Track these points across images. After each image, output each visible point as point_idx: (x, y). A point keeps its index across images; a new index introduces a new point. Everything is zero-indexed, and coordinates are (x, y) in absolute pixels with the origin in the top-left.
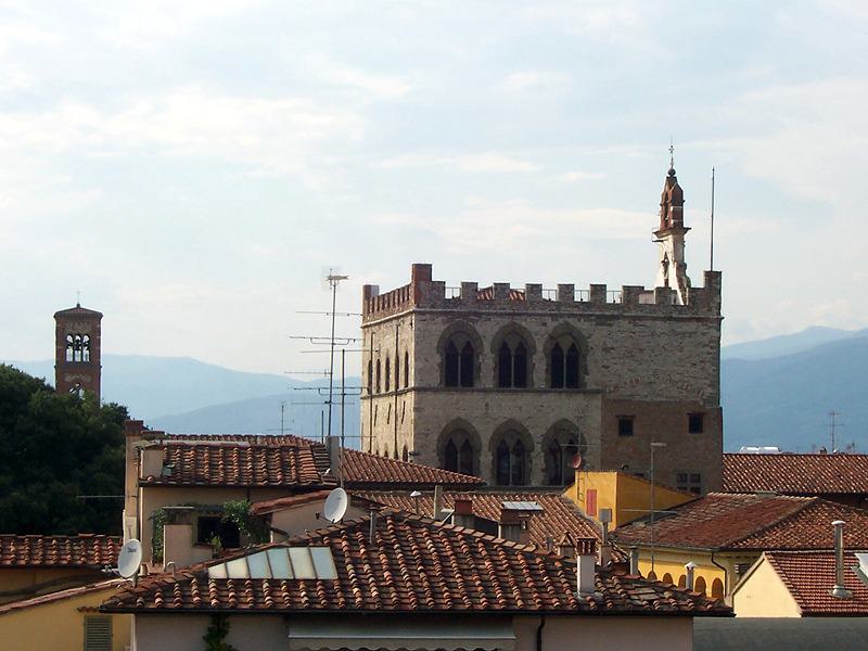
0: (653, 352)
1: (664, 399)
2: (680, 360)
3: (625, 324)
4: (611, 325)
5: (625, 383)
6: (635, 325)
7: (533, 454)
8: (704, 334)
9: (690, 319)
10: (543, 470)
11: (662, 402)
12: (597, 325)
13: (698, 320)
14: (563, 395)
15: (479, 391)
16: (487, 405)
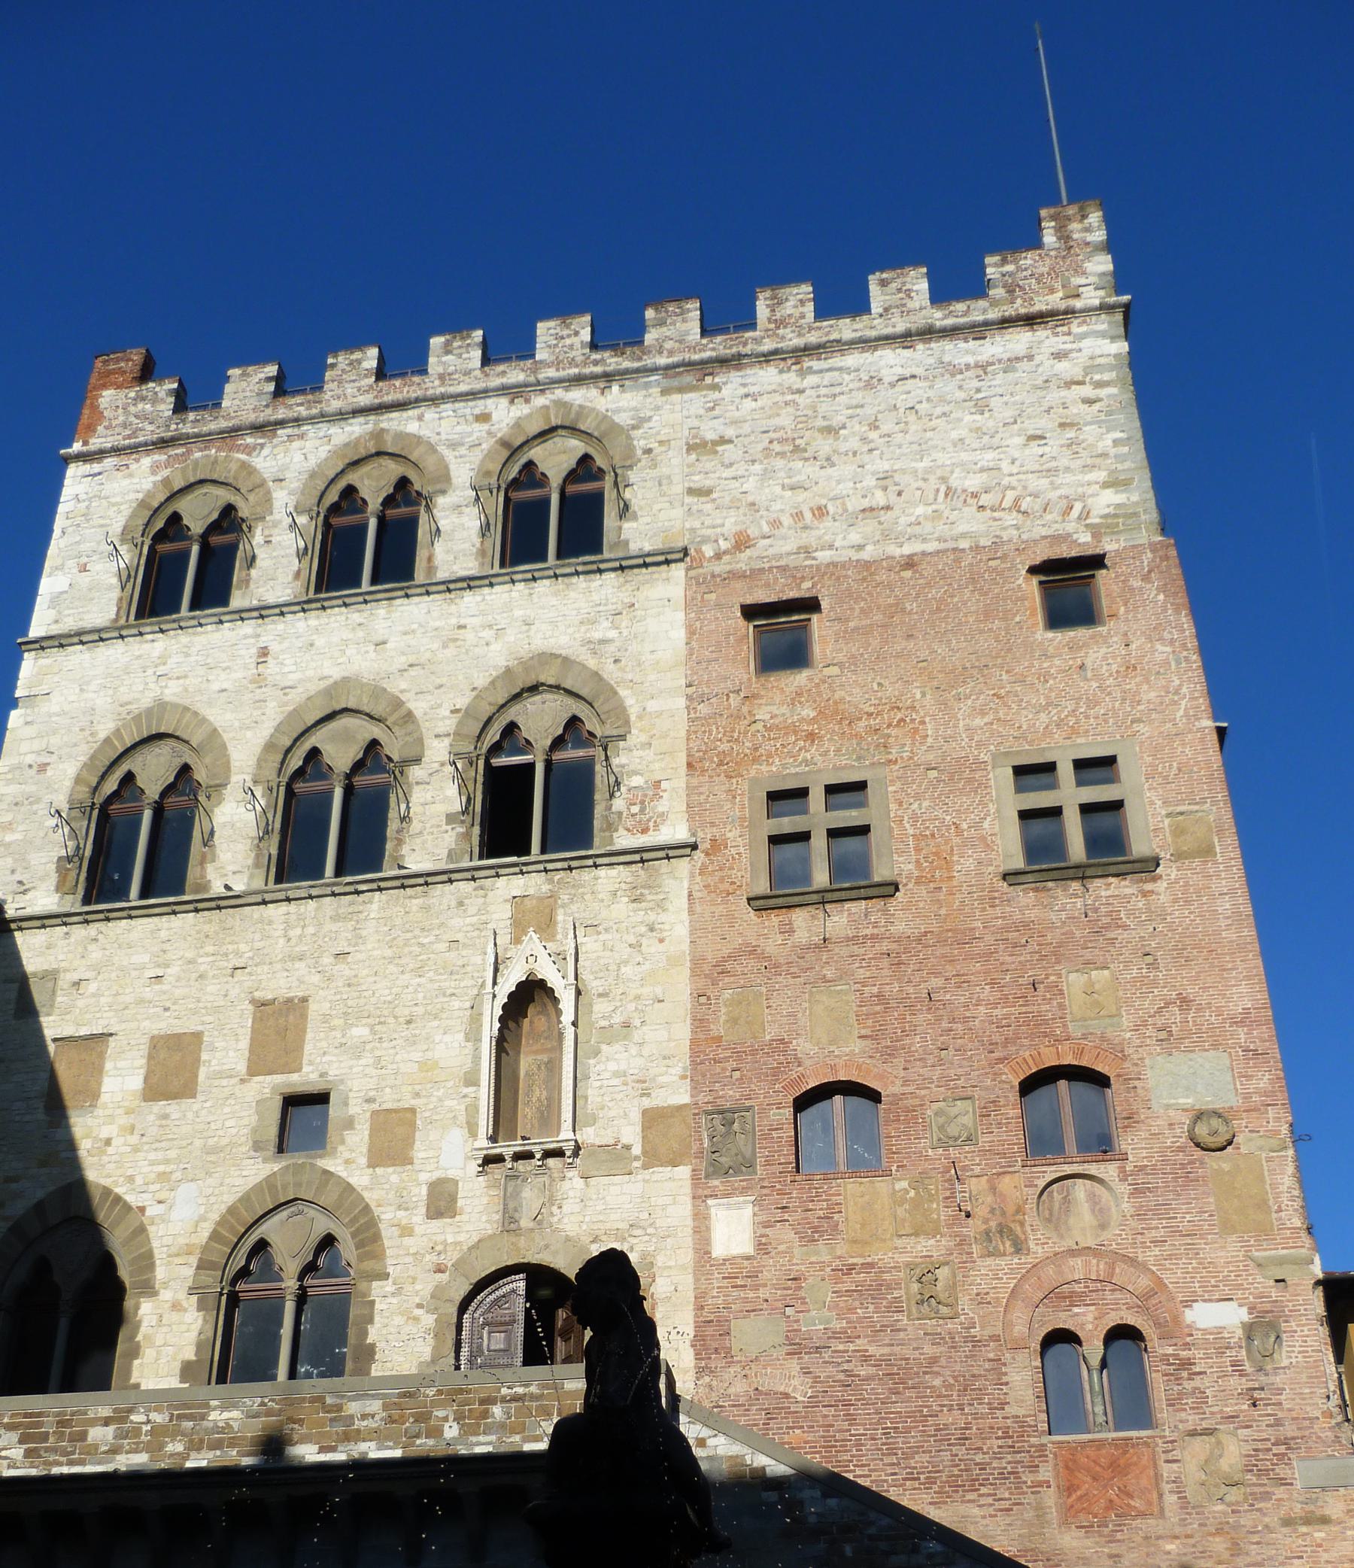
0: (874, 426)
1: (931, 547)
2: (978, 431)
4: (716, 387)
5: (776, 524)
6: (803, 373)
7: (415, 773)
8: (1059, 356)
9: (1006, 323)
10: (450, 818)
11: (924, 553)
12: (665, 392)
13: (1031, 320)
14: (543, 586)
15: (241, 615)
16: (264, 652)
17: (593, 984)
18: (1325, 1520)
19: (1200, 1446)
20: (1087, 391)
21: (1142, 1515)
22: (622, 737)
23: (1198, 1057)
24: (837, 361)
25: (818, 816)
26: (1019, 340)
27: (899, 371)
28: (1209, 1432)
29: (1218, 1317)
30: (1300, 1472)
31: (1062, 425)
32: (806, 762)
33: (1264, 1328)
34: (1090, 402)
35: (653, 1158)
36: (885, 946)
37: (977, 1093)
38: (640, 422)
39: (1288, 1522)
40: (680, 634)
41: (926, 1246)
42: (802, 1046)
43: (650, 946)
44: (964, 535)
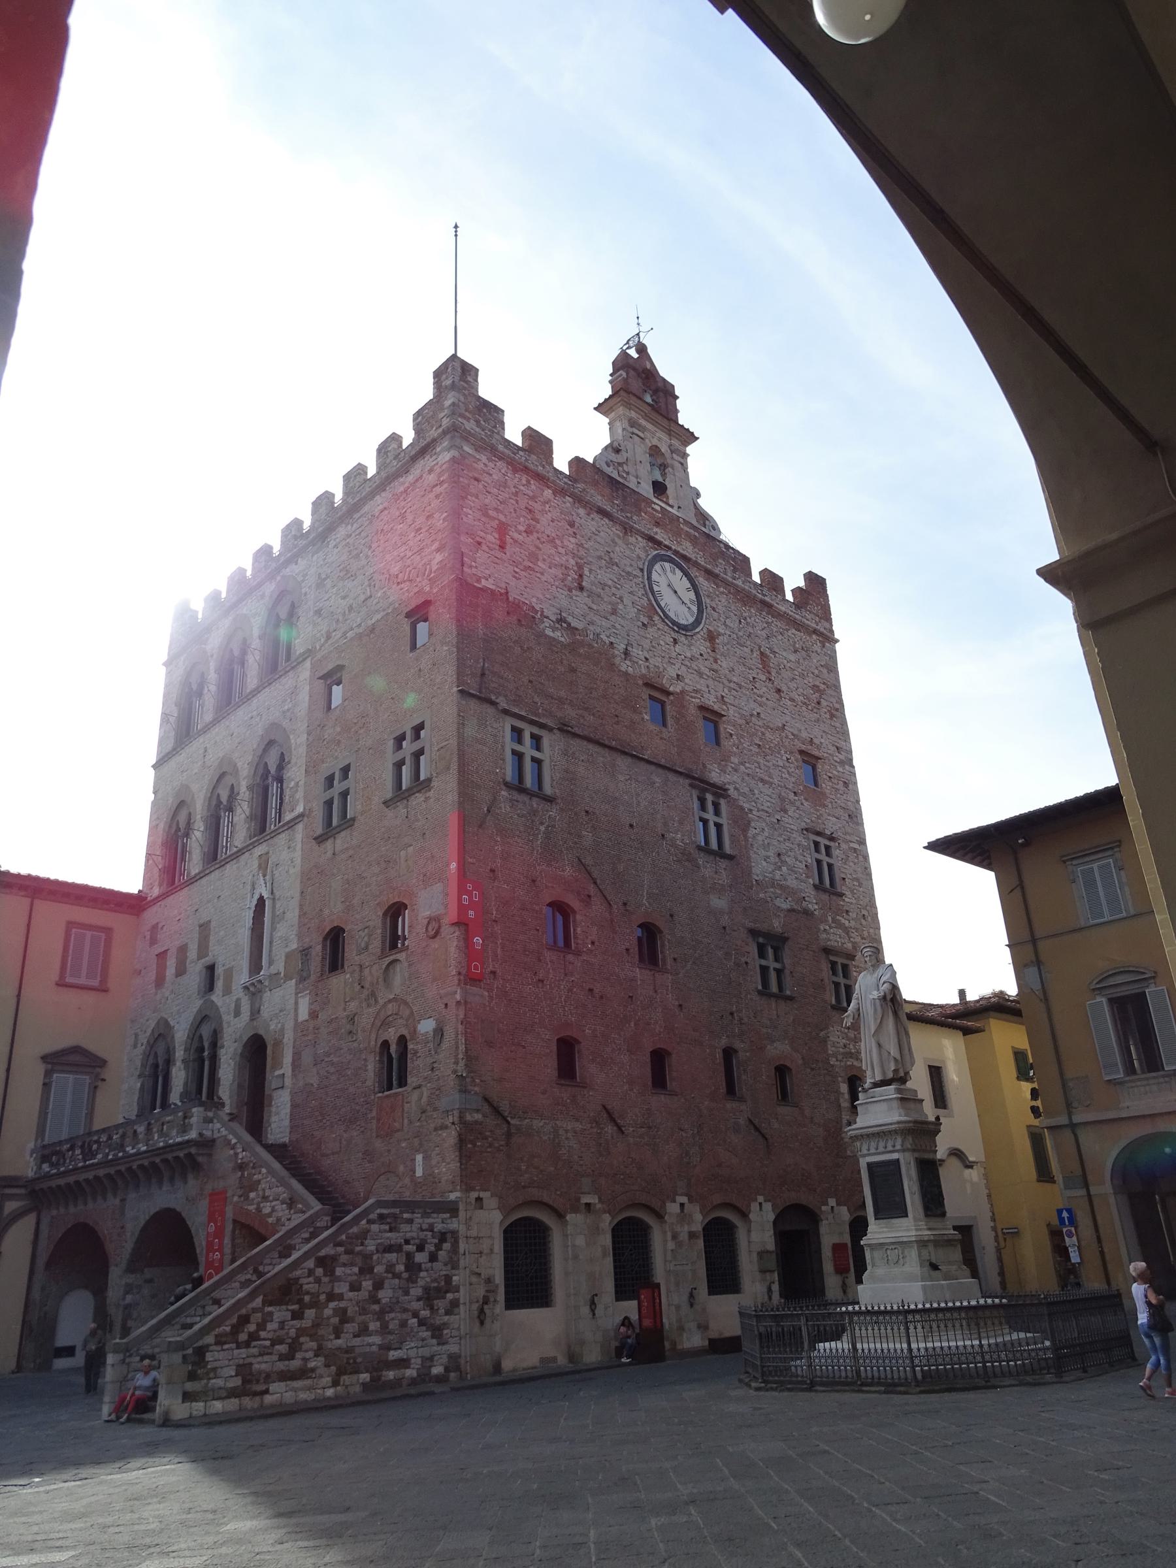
1: (379, 616)
2: (401, 535)
3: (342, 531)
11: (378, 621)
17: (277, 894)
18: (446, 1127)
19: (417, 1092)
20: (438, 490)
21: (398, 1131)
22: (289, 762)
24: (362, 512)
25: (338, 787)
26: (421, 463)
27: (381, 507)
28: (419, 1087)
29: (426, 1026)
31: (428, 517)
32: (337, 758)
33: (439, 1032)
34: (437, 497)
35: (288, 977)
36: (351, 852)
37: (371, 923)
39: (436, 1129)
40: (307, 698)
41: (353, 1006)
42: (326, 912)
44: (391, 604)
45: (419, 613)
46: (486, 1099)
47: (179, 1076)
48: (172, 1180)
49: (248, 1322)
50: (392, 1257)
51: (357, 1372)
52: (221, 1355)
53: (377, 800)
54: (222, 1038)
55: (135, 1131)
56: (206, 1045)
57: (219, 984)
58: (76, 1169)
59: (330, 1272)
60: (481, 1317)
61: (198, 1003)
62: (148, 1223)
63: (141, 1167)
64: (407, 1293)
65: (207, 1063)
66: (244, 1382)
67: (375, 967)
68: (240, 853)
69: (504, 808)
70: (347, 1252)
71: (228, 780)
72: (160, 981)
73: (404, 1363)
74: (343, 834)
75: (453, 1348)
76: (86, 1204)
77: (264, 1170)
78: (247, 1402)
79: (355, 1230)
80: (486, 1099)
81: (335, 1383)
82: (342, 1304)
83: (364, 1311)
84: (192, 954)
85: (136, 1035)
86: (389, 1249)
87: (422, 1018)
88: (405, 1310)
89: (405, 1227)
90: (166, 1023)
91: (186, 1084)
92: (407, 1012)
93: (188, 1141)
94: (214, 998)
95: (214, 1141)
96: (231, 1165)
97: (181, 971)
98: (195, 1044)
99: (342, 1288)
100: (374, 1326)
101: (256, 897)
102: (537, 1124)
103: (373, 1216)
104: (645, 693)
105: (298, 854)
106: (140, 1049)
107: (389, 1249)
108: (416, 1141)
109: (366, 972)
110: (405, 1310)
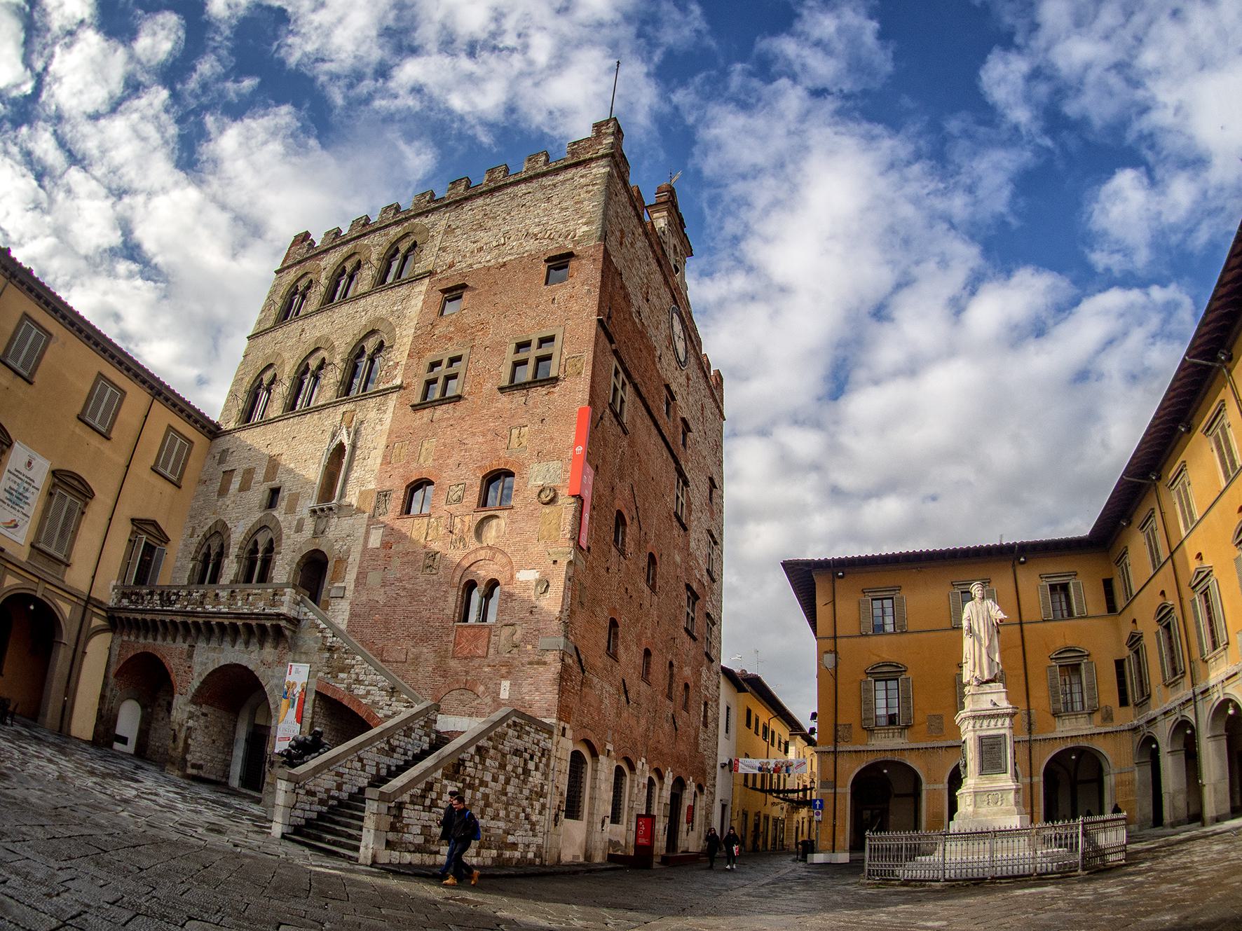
3: (480, 202)
17: (359, 444)
18: (545, 663)
23: (551, 464)
29: (528, 576)
30: (543, 643)
36: (452, 422)
38: (433, 225)
39: (530, 663)
43: (378, 427)
45: (560, 263)
46: (576, 649)
47: (231, 568)
48: (247, 643)
49: (431, 789)
50: (516, 759)
51: (490, 848)
52: (412, 814)
53: (490, 386)
54: (280, 546)
55: (217, 595)
56: (261, 549)
57: (282, 505)
58: (153, 611)
59: (483, 761)
60: (556, 820)
61: (257, 516)
62: (215, 671)
63: (220, 625)
64: (521, 792)
65: (259, 563)
66: (426, 841)
67: (467, 519)
68: (324, 407)
69: (607, 423)
70: (495, 748)
71: (323, 354)
72: (223, 491)
73: (514, 846)
74: (444, 407)
75: (540, 841)
76: (155, 639)
77: (359, 658)
78: (426, 856)
79: (499, 729)
80: (576, 649)
81: (478, 854)
82: (487, 791)
83: (498, 800)
84: (259, 475)
85: (194, 529)
86: (517, 752)
87: (521, 568)
88: (519, 805)
89: (526, 738)
90: (225, 525)
91: (236, 575)
92: (505, 560)
93: (278, 615)
94: (275, 513)
95: (299, 621)
96: (317, 646)
97: (244, 487)
98: (250, 546)
99: (488, 778)
100: (502, 813)
101: (337, 442)
102: (596, 680)
103: (510, 722)
104: (665, 392)
105: (388, 417)
106: (196, 540)
107: (517, 752)
108: (504, 670)
109: (457, 520)
110: (519, 805)
